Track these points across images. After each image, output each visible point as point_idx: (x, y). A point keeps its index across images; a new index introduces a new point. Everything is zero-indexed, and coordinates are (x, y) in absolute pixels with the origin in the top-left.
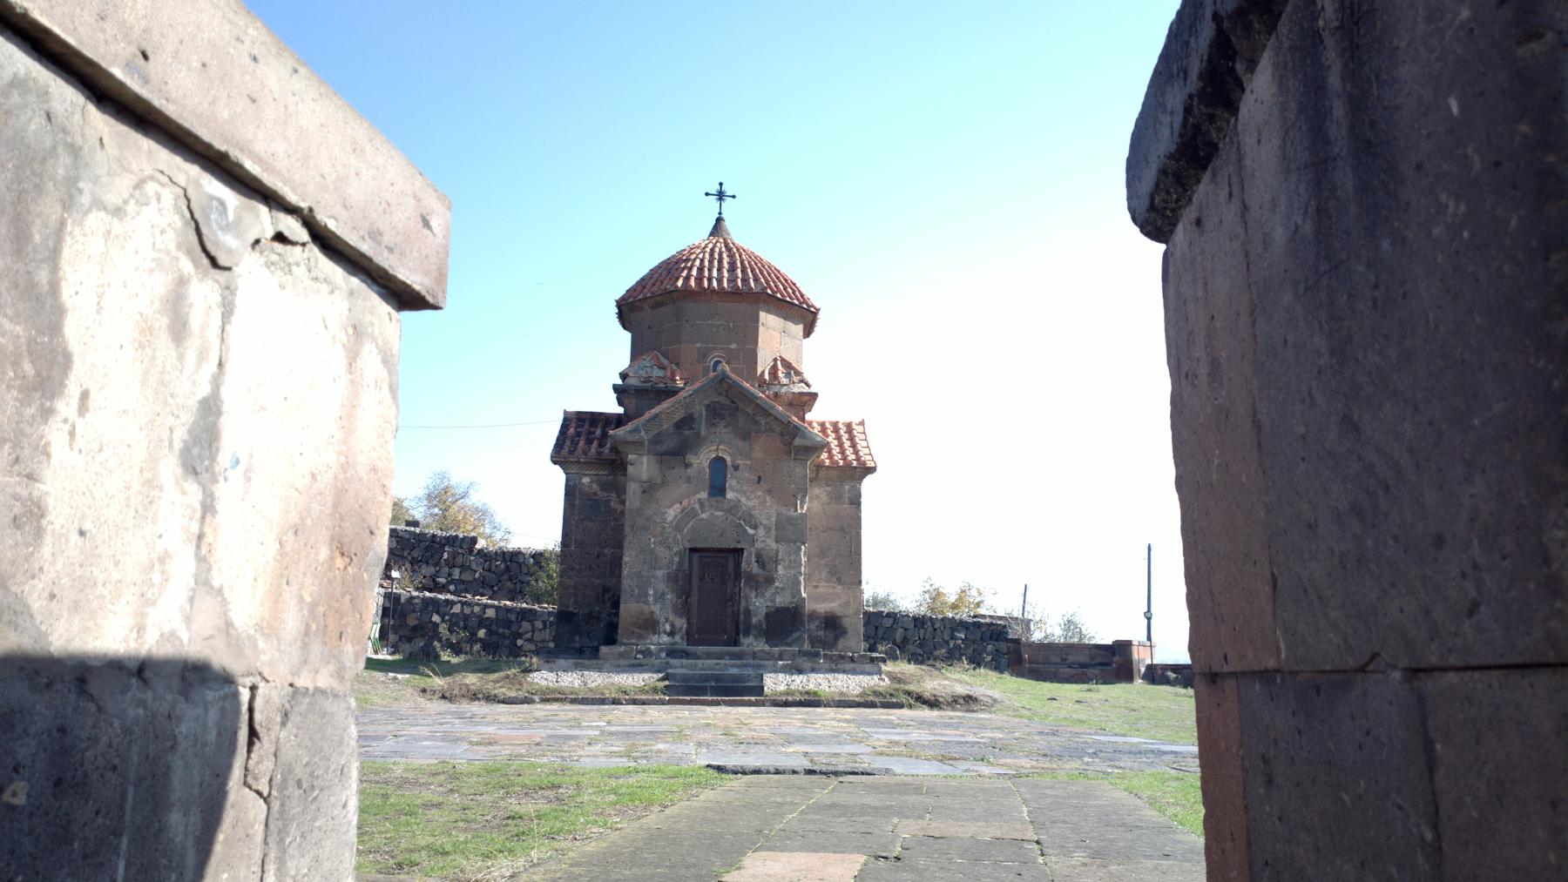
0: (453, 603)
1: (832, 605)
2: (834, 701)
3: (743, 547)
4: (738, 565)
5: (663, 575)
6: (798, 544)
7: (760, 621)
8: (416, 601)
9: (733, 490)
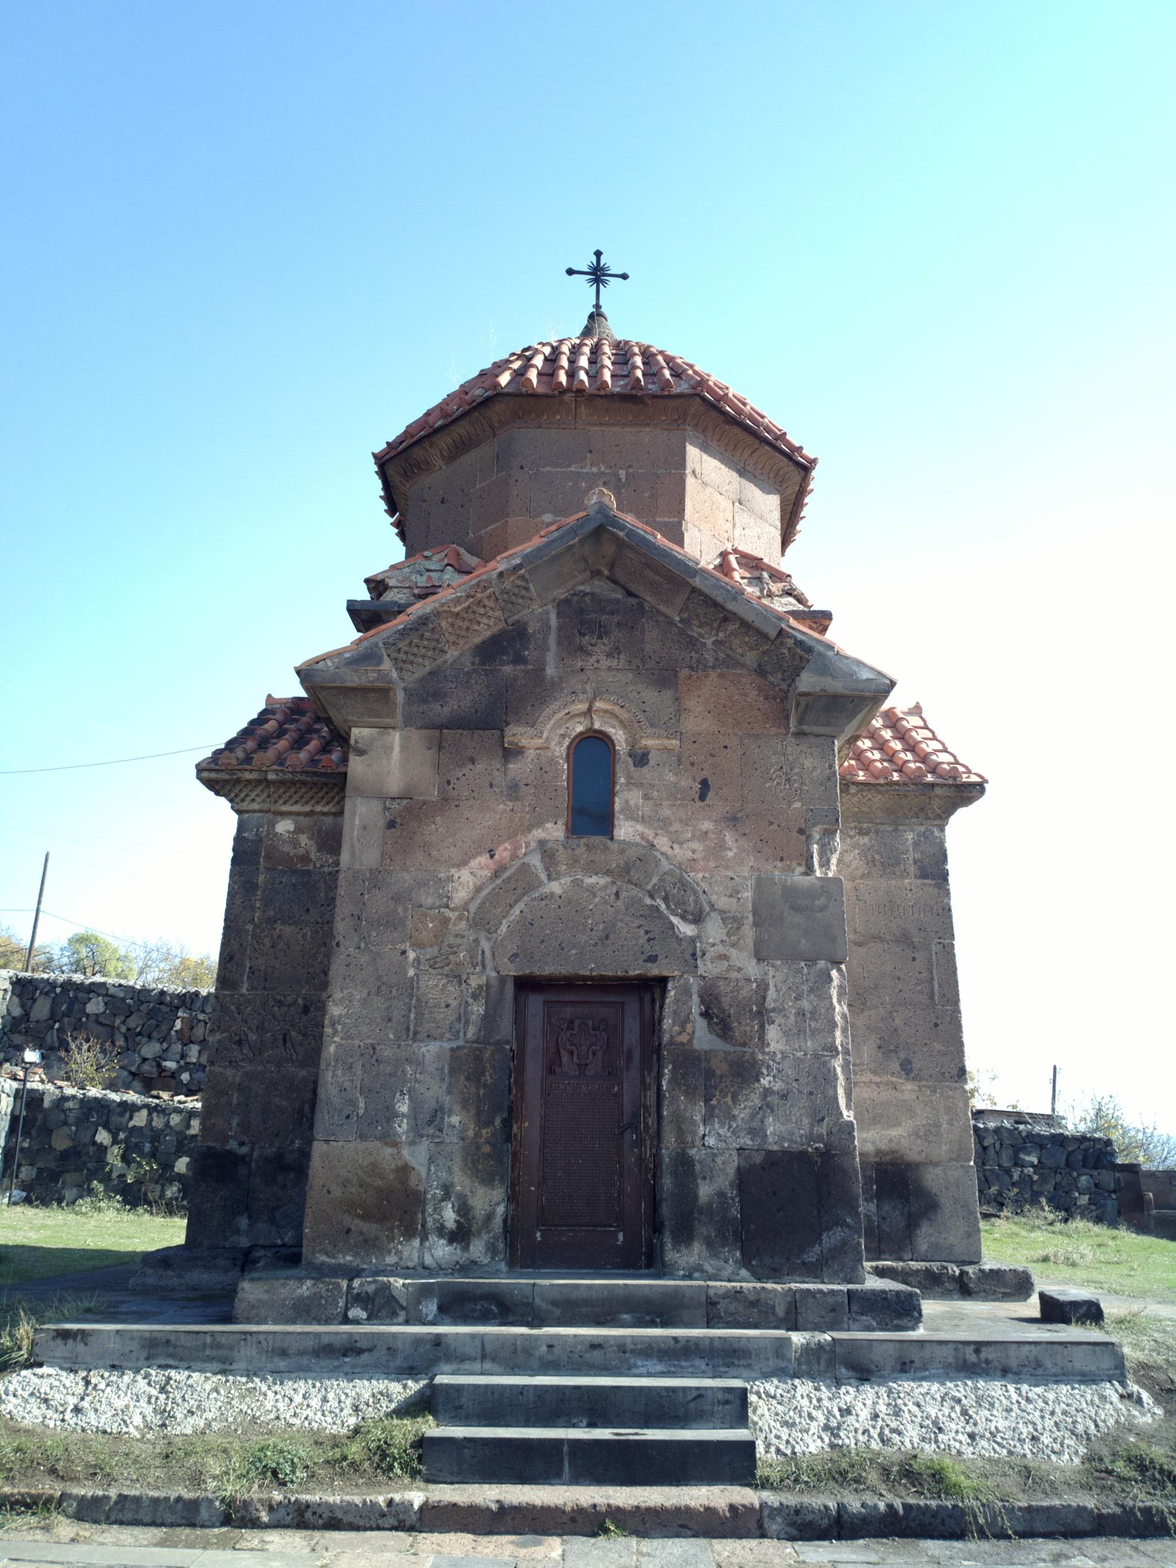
0: (128, 1109)
1: (895, 1132)
2: (1011, 1511)
3: (665, 973)
4: (652, 1027)
5: (438, 1057)
6: (822, 964)
7: (721, 1194)
8: (70, 1104)
9: (632, 816)
